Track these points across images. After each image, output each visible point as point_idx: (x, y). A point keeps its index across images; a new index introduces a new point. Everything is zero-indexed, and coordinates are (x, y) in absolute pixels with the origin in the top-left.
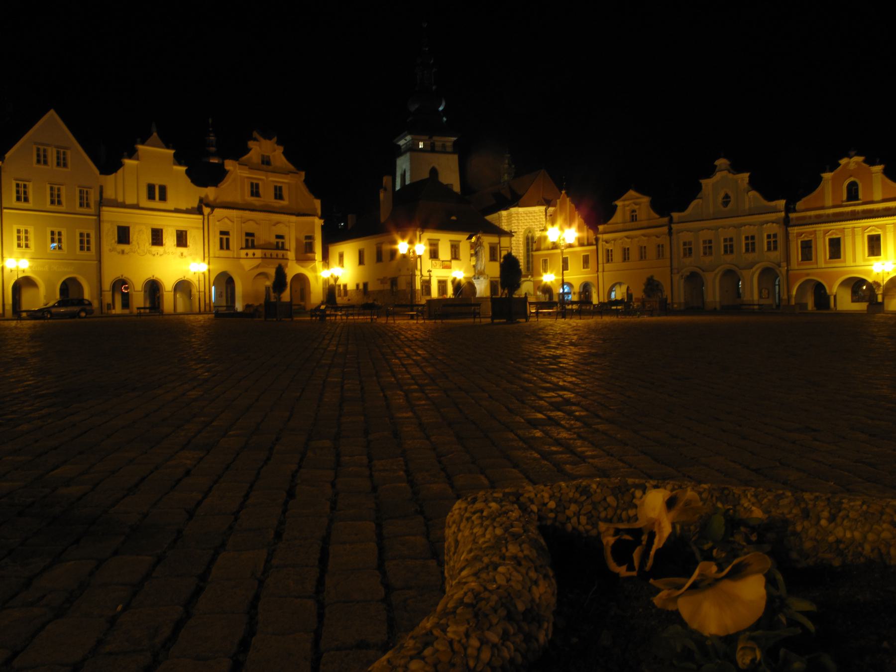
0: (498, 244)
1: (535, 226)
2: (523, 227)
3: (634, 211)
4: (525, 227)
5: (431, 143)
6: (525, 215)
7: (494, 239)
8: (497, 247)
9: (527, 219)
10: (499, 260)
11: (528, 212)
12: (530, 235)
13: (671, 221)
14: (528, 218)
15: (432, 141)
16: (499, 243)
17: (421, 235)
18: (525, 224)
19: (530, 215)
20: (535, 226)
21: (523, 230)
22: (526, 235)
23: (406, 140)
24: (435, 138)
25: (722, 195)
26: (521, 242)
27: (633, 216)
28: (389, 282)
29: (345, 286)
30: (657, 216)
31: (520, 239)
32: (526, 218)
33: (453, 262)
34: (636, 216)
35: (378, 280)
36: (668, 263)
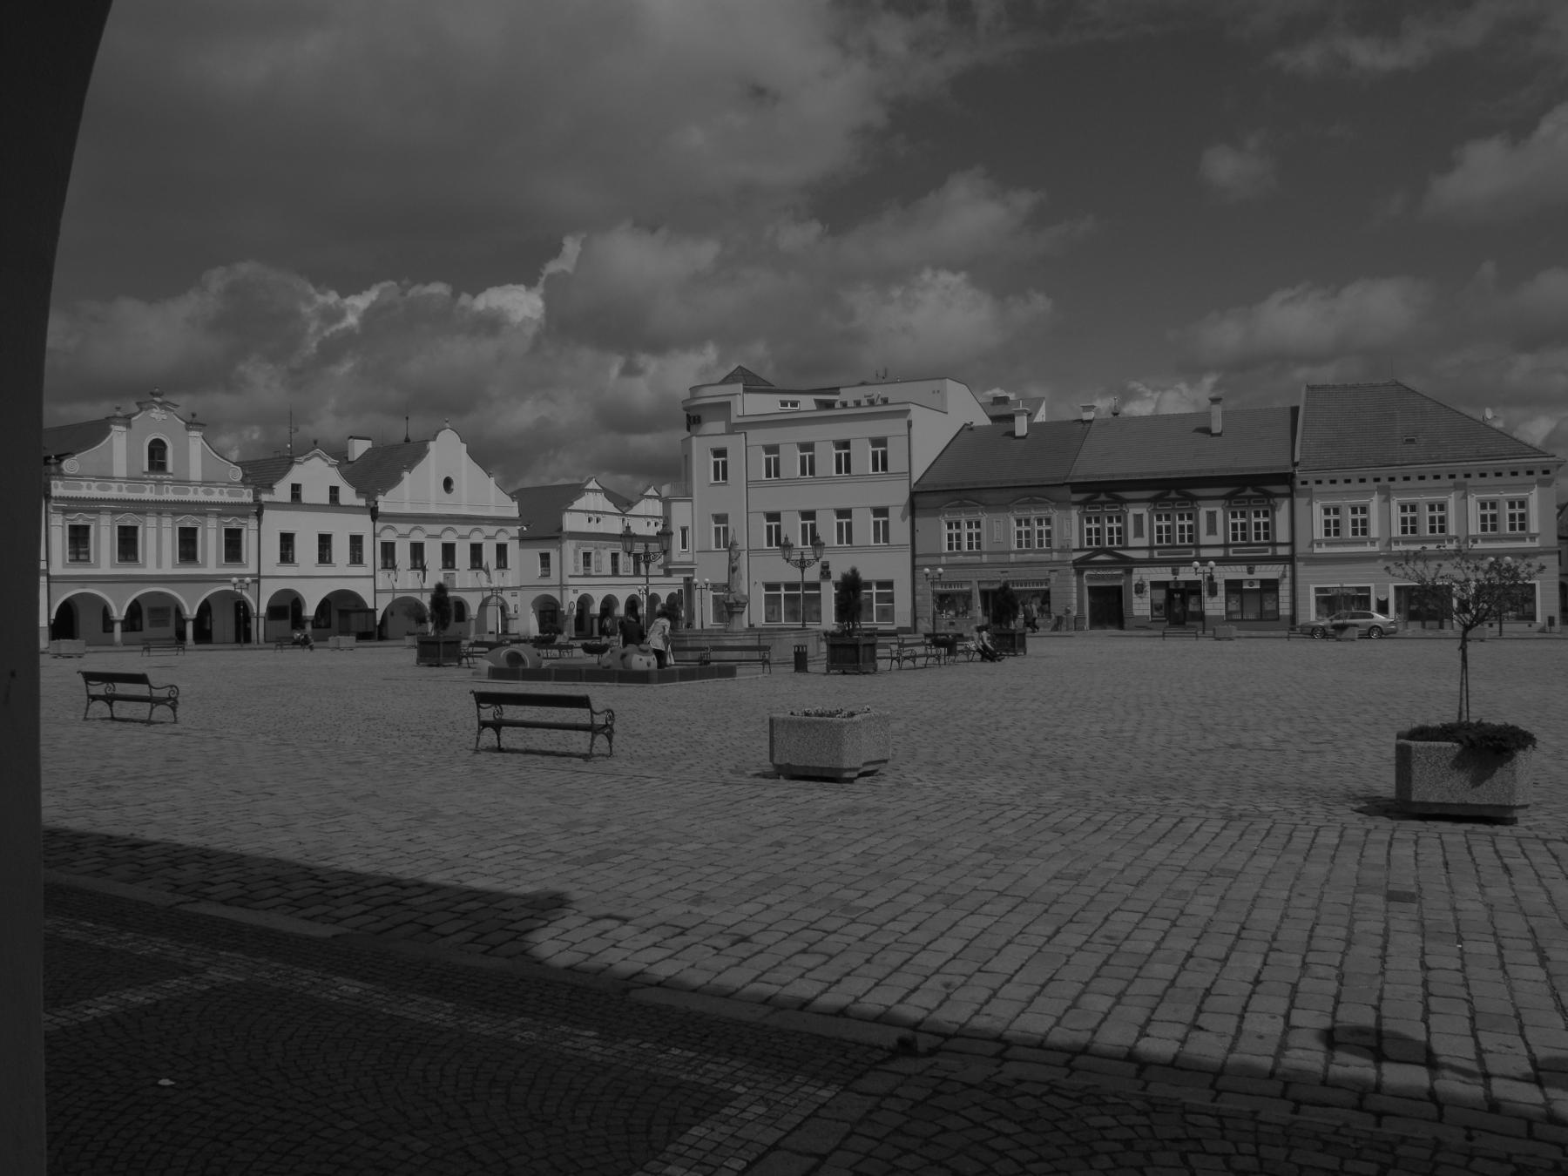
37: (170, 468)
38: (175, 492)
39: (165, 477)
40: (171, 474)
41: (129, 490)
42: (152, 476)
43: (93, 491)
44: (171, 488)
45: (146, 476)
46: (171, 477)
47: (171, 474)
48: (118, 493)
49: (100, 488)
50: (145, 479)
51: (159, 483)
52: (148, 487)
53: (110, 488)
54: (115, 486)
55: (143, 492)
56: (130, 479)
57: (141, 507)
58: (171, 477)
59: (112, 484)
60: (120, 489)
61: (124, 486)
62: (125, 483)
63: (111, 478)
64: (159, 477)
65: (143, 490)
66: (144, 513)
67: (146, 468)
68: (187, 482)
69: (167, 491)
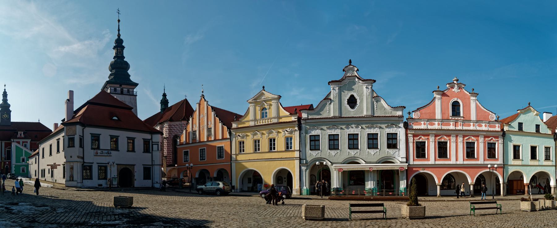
0: (150, 140)
2: (172, 134)
4: (174, 134)
6: (174, 127)
7: (148, 136)
8: (149, 142)
9: (175, 129)
10: (151, 152)
11: (175, 125)
14: (175, 128)
16: (152, 139)
17: (84, 130)
18: (174, 132)
19: (177, 126)
21: (172, 136)
22: (174, 139)
26: (171, 144)
31: (170, 142)
32: (174, 128)
33: (114, 153)
35: (48, 165)
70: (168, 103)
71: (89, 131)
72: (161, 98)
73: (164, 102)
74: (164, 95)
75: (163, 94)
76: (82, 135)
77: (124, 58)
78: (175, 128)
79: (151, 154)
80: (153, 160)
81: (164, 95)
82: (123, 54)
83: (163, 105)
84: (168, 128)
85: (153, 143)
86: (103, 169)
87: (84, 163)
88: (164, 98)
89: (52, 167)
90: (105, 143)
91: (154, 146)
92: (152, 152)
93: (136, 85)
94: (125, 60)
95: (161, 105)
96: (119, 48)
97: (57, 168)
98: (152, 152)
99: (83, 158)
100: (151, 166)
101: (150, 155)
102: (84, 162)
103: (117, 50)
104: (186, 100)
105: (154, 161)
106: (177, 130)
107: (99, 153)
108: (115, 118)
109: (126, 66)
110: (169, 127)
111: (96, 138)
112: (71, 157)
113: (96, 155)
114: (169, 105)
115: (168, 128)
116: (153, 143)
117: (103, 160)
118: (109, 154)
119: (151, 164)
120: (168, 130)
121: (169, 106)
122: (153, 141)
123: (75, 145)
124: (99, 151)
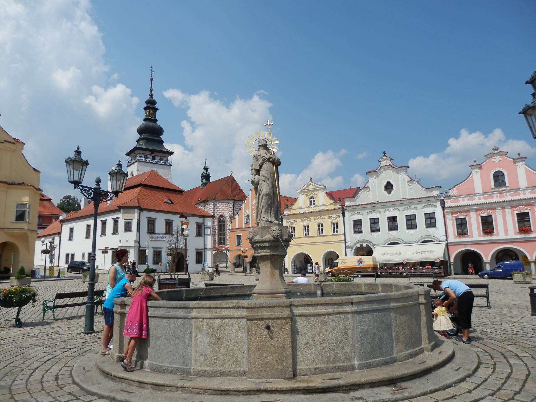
0: (202, 223)
1: (226, 214)
3: (312, 198)
4: (219, 214)
5: (153, 157)
7: (200, 220)
10: (203, 235)
12: (222, 219)
13: (343, 206)
14: (221, 208)
15: (154, 156)
20: (226, 214)
21: (217, 216)
23: (135, 154)
24: (155, 154)
25: (385, 184)
26: (216, 225)
27: (311, 202)
28: (110, 252)
29: (73, 255)
30: (332, 202)
33: (167, 237)
34: (314, 201)
36: (342, 237)
37: (507, 184)
38: (511, 195)
39: (504, 189)
40: (508, 187)
41: (484, 198)
42: (497, 190)
43: (466, 202)
44: (508, 194)
45: (493, 190)
46: (508, 188)
47: (508, 187)
48: (479, 201)
49: (469, 200)
50: (493, 192)
51: (501, 193)
52: (495, 195)
53: (474, 199)
54: (476, 198)
55: (493, 198)
56: (484, 193)
57: (492, 206)
58: (508, 188)
59: (475, 197)
60: (479, 199)
61: (482, 197)
62: (482, 195)
63: (474, 194)
64: (501, 189)
65: (493, 197)
66: (494, 209)
67: (493, 186)
68: (519, 189)
69: (507, 196)
70: (210, 177)
71: (146, 215)
72: (202, 171)
73: (206, 177)
74: (206, 168)
75: (204, 167)
76: (139, 219)
77: (157, 121)
78: (221, 208)
79: (203, 238)
80: (205, 244)
81: (206, 168)
82: (155, 117)
83: (205, 179)
84: (213, 207)
85: (205, 227)
86: (157, 254)
87: (139, 248)
88: (205, 171)
89: (103, 251)
90: (160, 227)
91: (206, 230)
92: (204, 235)
93: (171, 153)
94: (157, 123)
95: (202, 179)
96: (151, 110)
97: (108, 253)
98: (204, 235)
99: (139, 242)
100: (203, 250)
101: (203, 238)
102: (140, 246)
103: (149, 111)
104: (232, 177)
105: (206, 245)
106: (223, 210)
107: (154, 238)
108: (169, 202)
109: (159, 131)
110: (214, 206)
111: (151, 223)
112: (127, 241)
113: (152, 240)
114: (212, 180)
115: (213, 207)
116: (205, 227)
117: (157, 245)
118: (164, 238)
119: (203, 248)
120: (212, 210)
121: (211, 181)
122: (206, 225)
123: (133, 230)
124: (154, 236)
